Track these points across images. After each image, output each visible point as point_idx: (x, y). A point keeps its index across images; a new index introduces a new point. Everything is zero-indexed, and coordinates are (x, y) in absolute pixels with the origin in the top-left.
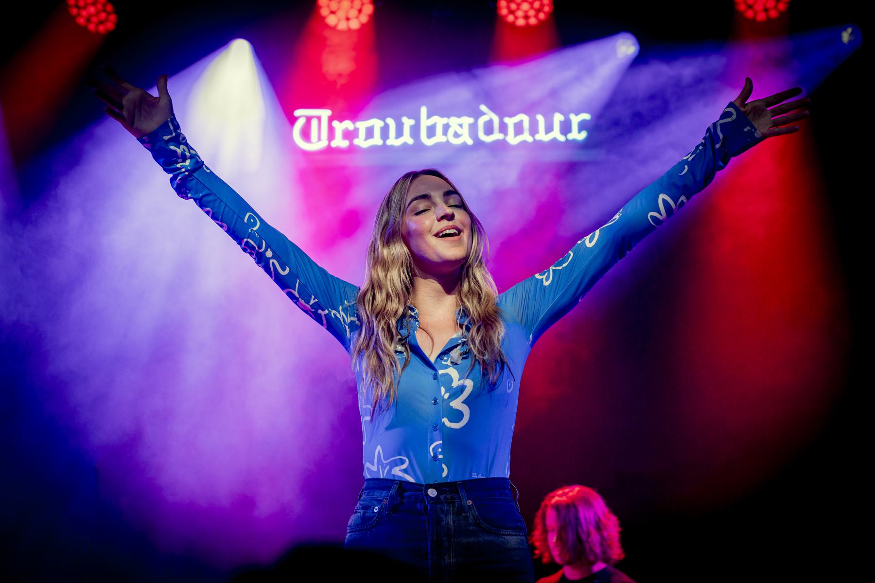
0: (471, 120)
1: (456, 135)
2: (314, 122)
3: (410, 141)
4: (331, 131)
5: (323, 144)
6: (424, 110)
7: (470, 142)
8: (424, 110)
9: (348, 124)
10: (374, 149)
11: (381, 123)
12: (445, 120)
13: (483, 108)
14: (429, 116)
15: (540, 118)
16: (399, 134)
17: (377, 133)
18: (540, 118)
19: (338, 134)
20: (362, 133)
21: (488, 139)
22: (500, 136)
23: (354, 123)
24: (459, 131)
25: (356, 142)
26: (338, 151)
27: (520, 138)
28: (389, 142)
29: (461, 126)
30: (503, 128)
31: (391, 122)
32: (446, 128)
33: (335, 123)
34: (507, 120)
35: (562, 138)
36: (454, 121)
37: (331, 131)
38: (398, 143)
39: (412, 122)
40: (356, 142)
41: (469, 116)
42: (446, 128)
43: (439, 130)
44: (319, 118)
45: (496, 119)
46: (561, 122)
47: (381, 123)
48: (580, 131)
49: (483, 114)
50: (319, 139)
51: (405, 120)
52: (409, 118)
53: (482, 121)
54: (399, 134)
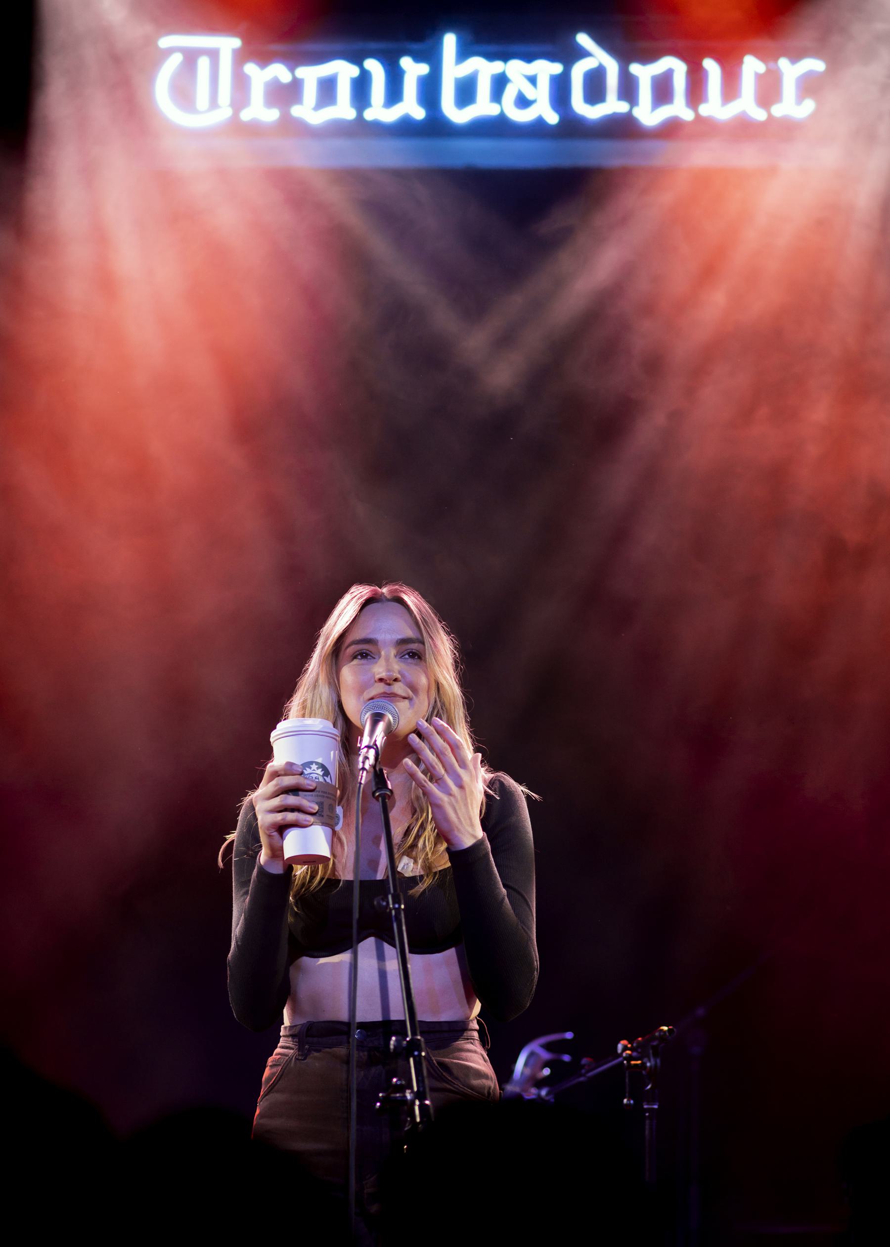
0: (557, 68)
1: (523, 102)
2: (203, 63)
3: (419, 114)
4: (241, 83)
5: (224, 113)
6: (450, 42)
7: (552, 118)
8: (450, 42)
9: (279, 71)
10: (339, 129)
11: (354, 71)
12: (498, 66)
13: (583, 39)
14: (463, 54)
15: (710, 65)
16: (394, 94)
17: (344, 91)
18: (710, 65)
19: (257, 92)
20: (310, 92)
21: (592, 113)
22: (623, 107)
23: (292, 70)
24: (530, 93)
25: (297, 111)
26: (254, 130)
27: (665, 113)
28: (369, 115)
29: (533, 80)
30: (628, 90)
31: (374, 66)
32: (500, 83)
33: (251, 68)
34: (635, 68)
35: (759, 115)
36: (516, 68)
37: (241, 83)
38: (391, 115)
39: (423, 69)
40: (297, 111)
41: (552, 57)
42: (500, 83)
43: (484, 89)
44: (213, 54)
45: (612, 67)
46: (759, 77)
47: (355, 71)
48: (800, 99)
49: (583, 54)
50: (214, 103)
51: (406, 62)
52: (418, 57)
53: (579, 70)
54: (394, 94)
